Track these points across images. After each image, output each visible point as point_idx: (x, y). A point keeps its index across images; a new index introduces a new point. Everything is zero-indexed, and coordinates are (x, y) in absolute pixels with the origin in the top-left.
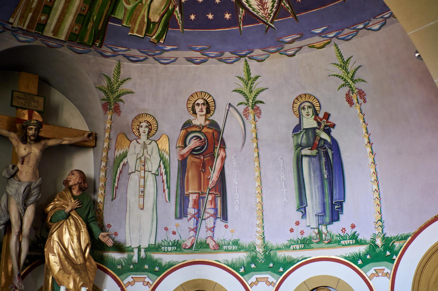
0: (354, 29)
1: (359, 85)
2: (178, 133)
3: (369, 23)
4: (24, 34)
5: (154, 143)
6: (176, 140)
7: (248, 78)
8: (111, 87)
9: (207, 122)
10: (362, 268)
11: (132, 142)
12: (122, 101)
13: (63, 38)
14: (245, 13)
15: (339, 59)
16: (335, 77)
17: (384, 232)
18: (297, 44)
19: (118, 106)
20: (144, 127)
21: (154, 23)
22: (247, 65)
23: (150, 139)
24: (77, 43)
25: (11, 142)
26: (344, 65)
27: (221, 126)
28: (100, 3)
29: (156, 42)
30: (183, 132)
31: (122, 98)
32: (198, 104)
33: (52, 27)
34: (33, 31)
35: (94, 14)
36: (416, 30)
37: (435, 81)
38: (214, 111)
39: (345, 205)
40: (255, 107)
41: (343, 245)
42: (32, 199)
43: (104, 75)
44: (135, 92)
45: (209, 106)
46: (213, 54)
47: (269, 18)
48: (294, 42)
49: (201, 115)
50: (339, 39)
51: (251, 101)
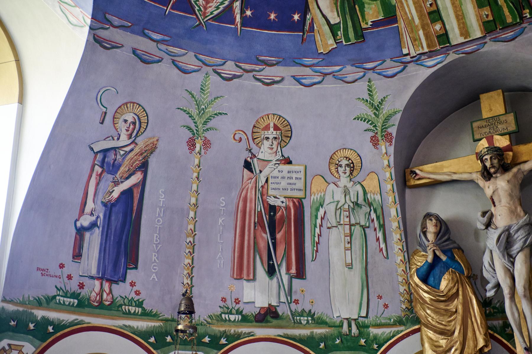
13: (479, 34)
24: (500, 29)
25: (478, 184)
33: (457, 31)
34: (438, 48)
42: (517, 246)
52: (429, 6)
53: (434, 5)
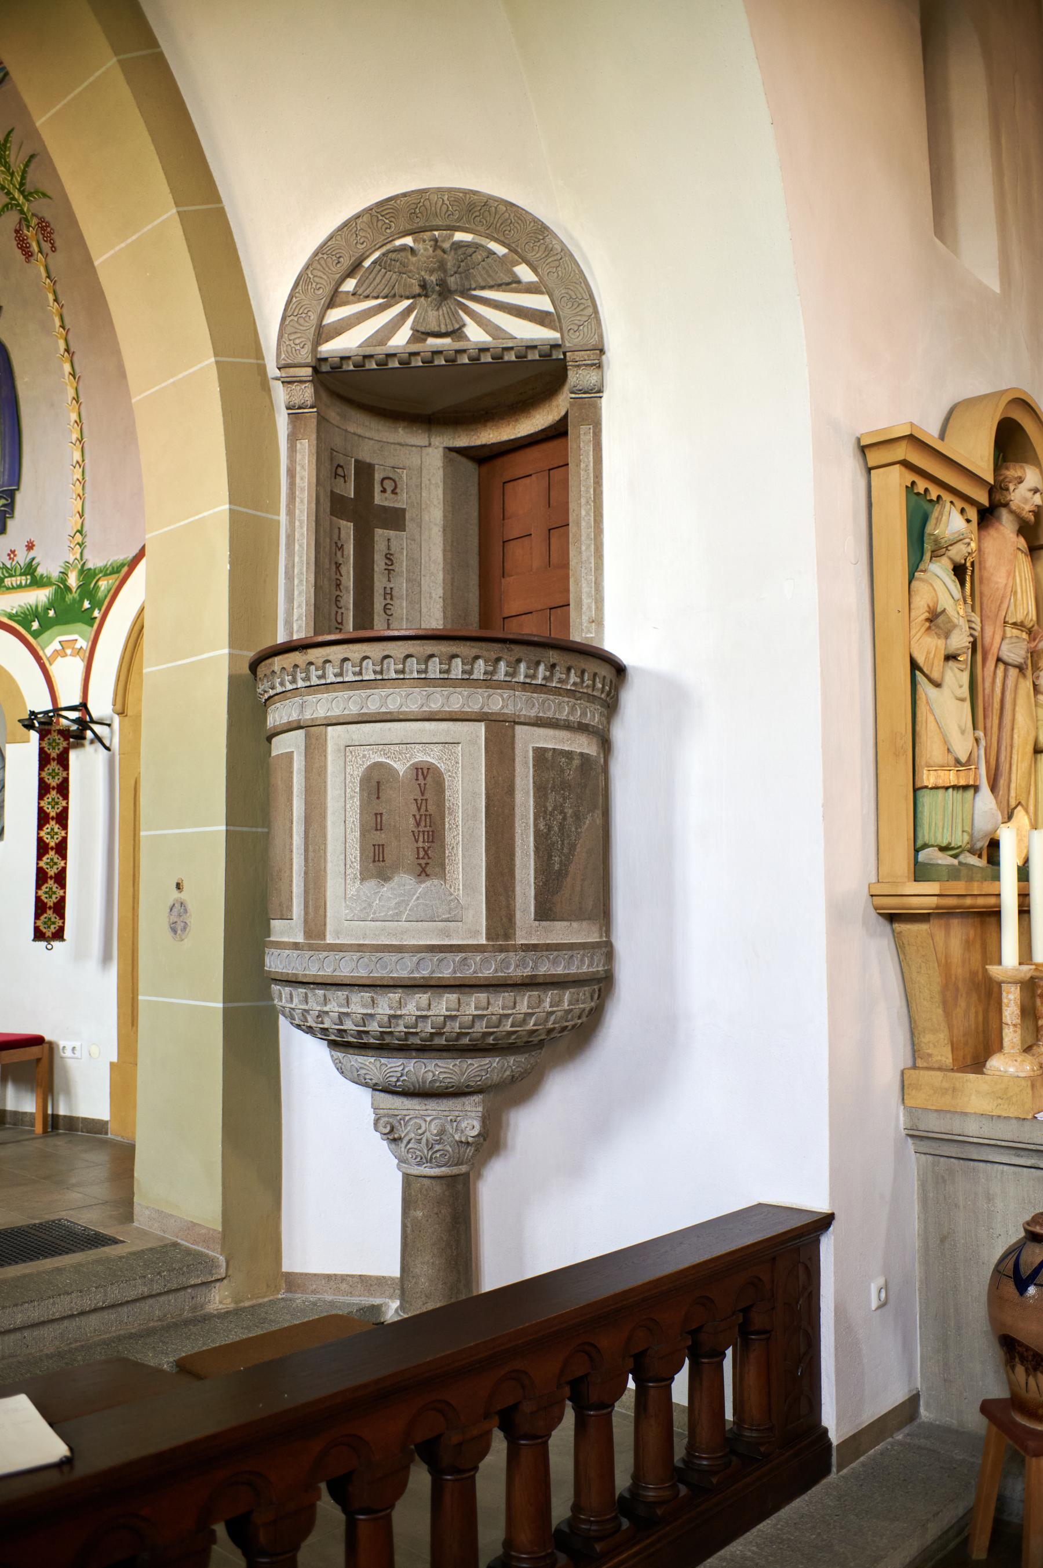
10: (39, 639)
17: (85, 557)
39: (19, 497)
41: (8, 588)
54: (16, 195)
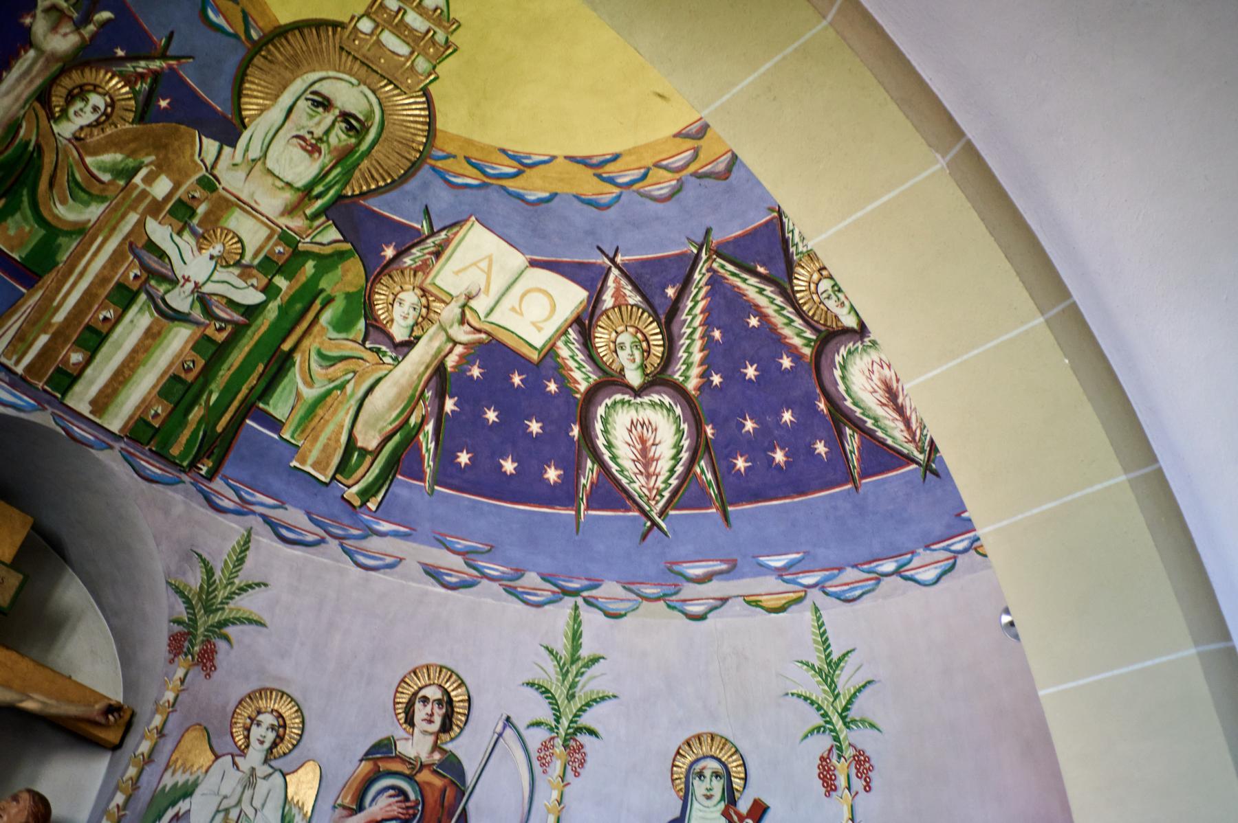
0: (869, 572)
1: (859, 737)
2: (352, 767)
3: (910, 561)
4: (12, 385)
5: (277, 777)
6: (340, 785)
7: (573, 655)
8: (208, 593)
9: (437, 756)
11: (220, 760)
12: (226, 638)
13: (115, 426)
14: (598, 475)
15: (819, 651)
16: (801, 701)
18: (716, 588)
19: (214, 651)
20: (264, 726)
21: (364, 452)
22: (576, 617)
23: (273, 763)
24: (150, 450)
26: (829, 671)
27: (470, 778)
28: (236, 365)
29: (357, 502)
30: (366, 767)
31: (230, 630)
32: (425, 700)
33: (93, 391)
34: (40, 385)
35: (213, 386)
36: (1005, 523)
37: (1041, 693)
38: (462, 729)
40: (572, 743)
43: (200, 556)
44: (268, 623)
45: (453, 711)
46: (494, 569)
47: (657, 502)
48: (710, 580)
49: (425, 732)
50: (827, 594)
51: (565, 722)
52: (101, 317)
53: (108, 325)
54: (835, 718)
